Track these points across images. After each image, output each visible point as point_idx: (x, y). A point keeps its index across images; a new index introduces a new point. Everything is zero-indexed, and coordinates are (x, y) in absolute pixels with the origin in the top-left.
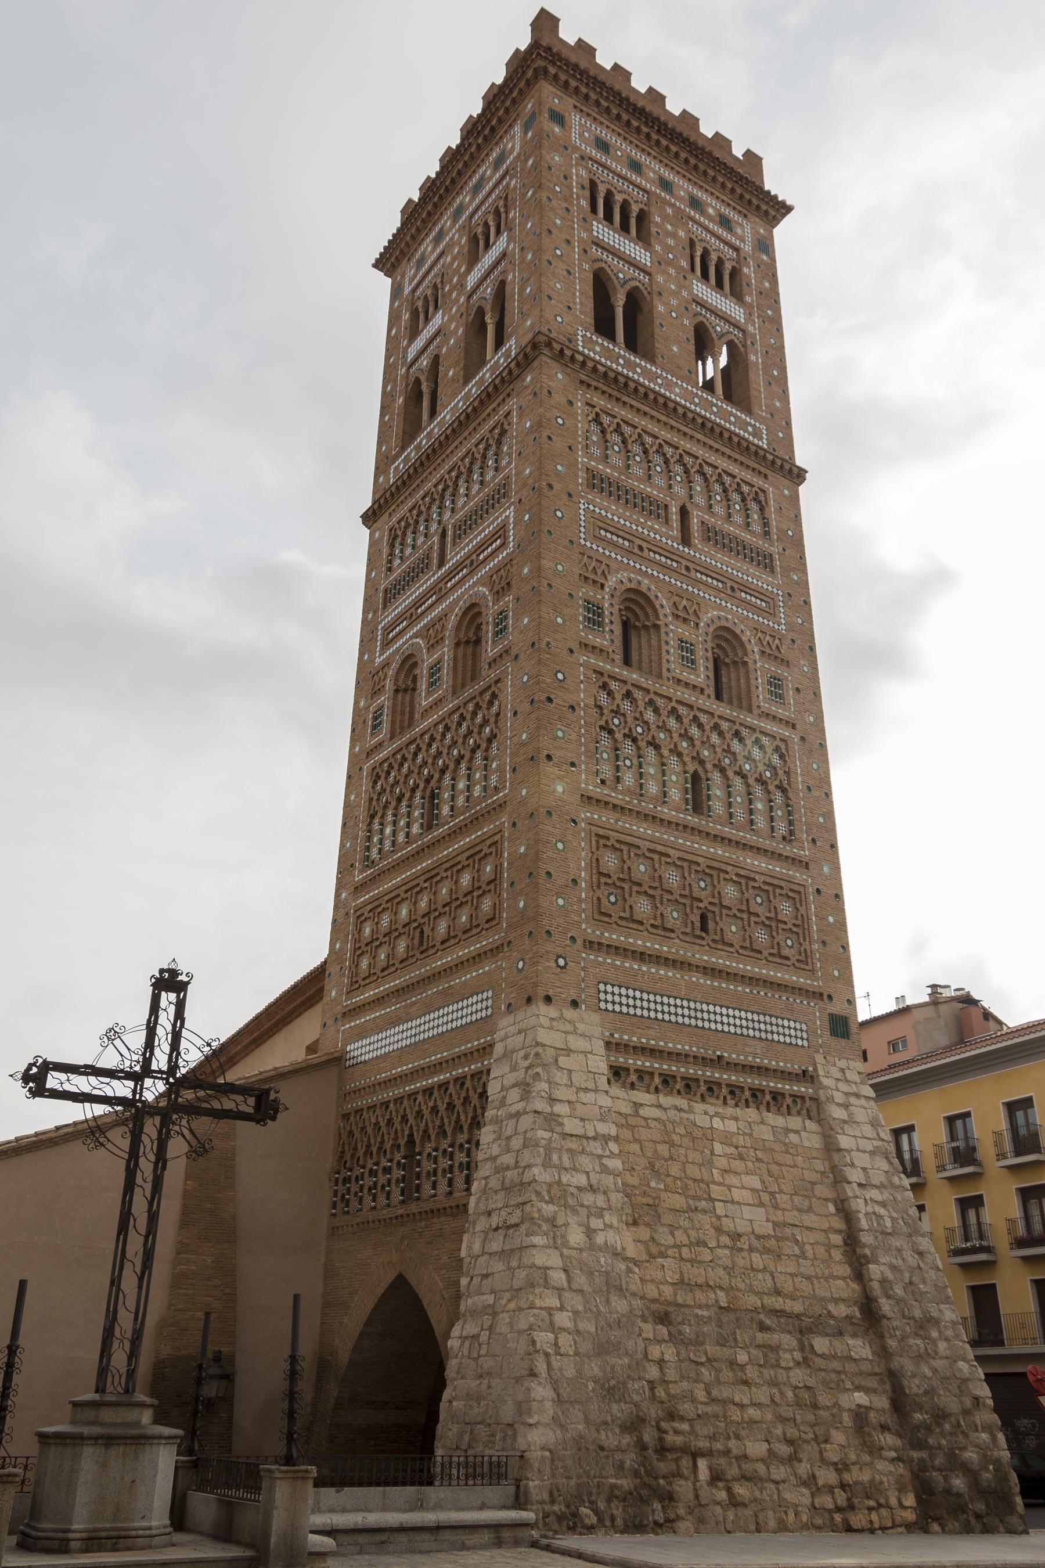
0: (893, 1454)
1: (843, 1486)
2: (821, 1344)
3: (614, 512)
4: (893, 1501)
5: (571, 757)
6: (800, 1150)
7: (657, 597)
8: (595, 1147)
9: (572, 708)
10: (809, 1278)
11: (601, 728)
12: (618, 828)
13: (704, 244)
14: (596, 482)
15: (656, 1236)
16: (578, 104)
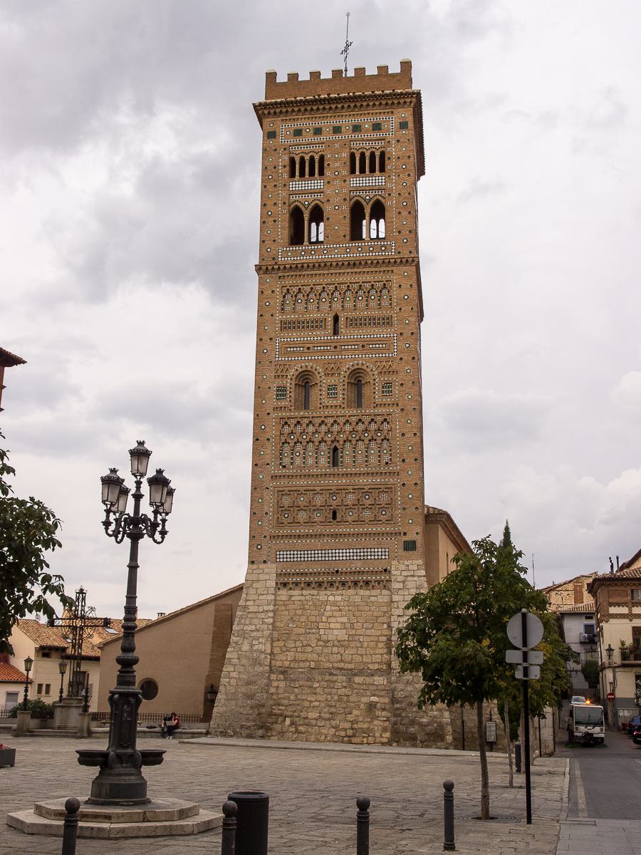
0: (385, 719)
1: (352, 729)
2: (358, 679)
3: (294, 336)
4: (377, 735)
5: (267, 461)
6: (375, 603)
7: (316, 369)
8: (263, 615)
9: (268, 439)
10: (362, 655)
11: (283, 443)
12: (289, 485)
13: (361, 151)
14: (286, 326)
15: (286, 644)
16: (284, 118)
